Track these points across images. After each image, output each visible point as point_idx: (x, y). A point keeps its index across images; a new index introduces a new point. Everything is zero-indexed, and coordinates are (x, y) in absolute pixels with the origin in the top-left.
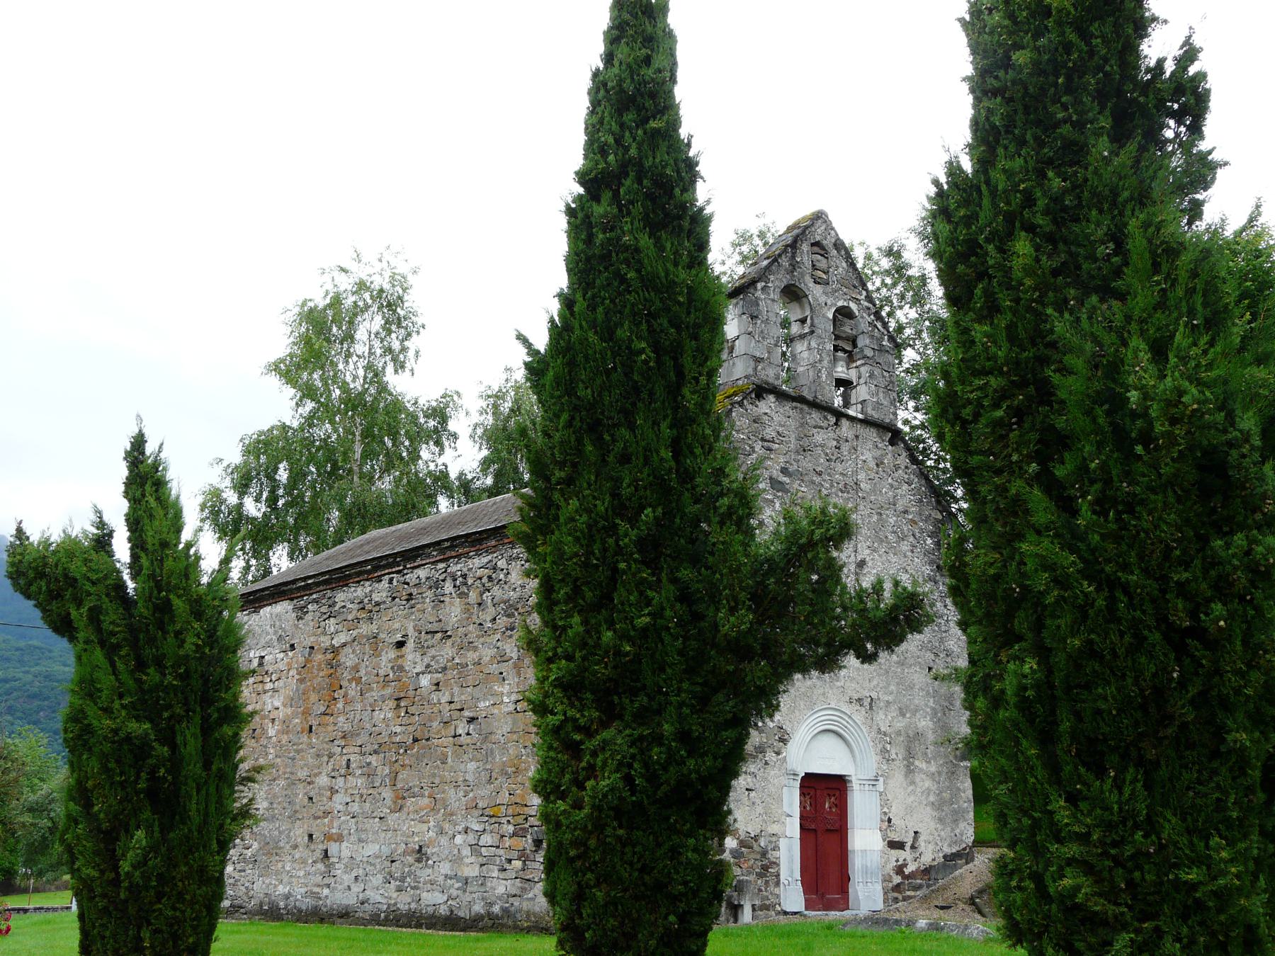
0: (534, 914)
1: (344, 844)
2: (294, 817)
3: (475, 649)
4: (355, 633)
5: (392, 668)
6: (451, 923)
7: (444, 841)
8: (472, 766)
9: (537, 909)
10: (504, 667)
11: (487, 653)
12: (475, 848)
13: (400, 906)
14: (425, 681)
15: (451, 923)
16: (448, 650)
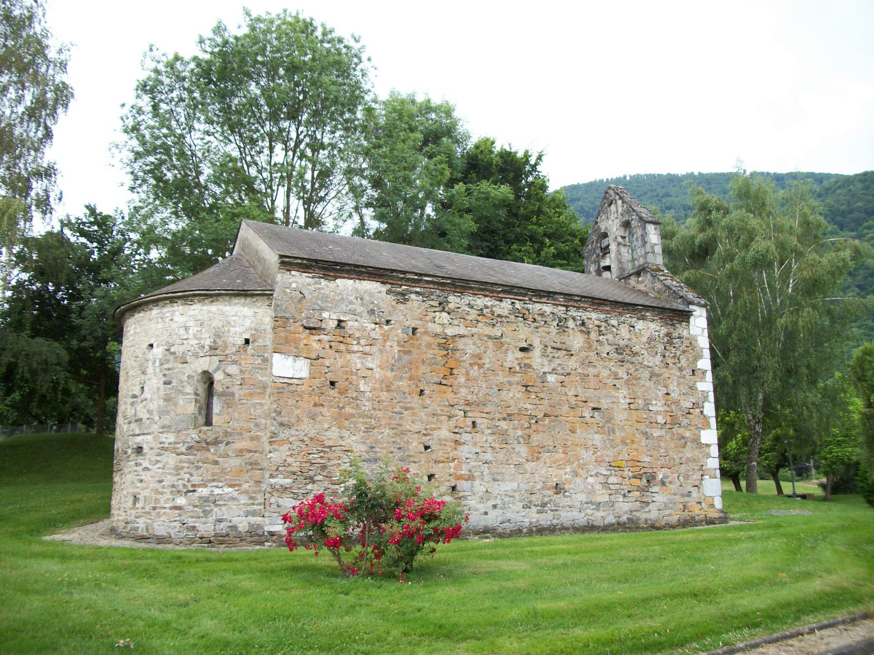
1: (477, 482)
3: (595, 366)
7: (578, 480)
8: (598, 437)
11: (605, 373)
12: (605, 485)
14: (551, 378)
16: (572, 363)
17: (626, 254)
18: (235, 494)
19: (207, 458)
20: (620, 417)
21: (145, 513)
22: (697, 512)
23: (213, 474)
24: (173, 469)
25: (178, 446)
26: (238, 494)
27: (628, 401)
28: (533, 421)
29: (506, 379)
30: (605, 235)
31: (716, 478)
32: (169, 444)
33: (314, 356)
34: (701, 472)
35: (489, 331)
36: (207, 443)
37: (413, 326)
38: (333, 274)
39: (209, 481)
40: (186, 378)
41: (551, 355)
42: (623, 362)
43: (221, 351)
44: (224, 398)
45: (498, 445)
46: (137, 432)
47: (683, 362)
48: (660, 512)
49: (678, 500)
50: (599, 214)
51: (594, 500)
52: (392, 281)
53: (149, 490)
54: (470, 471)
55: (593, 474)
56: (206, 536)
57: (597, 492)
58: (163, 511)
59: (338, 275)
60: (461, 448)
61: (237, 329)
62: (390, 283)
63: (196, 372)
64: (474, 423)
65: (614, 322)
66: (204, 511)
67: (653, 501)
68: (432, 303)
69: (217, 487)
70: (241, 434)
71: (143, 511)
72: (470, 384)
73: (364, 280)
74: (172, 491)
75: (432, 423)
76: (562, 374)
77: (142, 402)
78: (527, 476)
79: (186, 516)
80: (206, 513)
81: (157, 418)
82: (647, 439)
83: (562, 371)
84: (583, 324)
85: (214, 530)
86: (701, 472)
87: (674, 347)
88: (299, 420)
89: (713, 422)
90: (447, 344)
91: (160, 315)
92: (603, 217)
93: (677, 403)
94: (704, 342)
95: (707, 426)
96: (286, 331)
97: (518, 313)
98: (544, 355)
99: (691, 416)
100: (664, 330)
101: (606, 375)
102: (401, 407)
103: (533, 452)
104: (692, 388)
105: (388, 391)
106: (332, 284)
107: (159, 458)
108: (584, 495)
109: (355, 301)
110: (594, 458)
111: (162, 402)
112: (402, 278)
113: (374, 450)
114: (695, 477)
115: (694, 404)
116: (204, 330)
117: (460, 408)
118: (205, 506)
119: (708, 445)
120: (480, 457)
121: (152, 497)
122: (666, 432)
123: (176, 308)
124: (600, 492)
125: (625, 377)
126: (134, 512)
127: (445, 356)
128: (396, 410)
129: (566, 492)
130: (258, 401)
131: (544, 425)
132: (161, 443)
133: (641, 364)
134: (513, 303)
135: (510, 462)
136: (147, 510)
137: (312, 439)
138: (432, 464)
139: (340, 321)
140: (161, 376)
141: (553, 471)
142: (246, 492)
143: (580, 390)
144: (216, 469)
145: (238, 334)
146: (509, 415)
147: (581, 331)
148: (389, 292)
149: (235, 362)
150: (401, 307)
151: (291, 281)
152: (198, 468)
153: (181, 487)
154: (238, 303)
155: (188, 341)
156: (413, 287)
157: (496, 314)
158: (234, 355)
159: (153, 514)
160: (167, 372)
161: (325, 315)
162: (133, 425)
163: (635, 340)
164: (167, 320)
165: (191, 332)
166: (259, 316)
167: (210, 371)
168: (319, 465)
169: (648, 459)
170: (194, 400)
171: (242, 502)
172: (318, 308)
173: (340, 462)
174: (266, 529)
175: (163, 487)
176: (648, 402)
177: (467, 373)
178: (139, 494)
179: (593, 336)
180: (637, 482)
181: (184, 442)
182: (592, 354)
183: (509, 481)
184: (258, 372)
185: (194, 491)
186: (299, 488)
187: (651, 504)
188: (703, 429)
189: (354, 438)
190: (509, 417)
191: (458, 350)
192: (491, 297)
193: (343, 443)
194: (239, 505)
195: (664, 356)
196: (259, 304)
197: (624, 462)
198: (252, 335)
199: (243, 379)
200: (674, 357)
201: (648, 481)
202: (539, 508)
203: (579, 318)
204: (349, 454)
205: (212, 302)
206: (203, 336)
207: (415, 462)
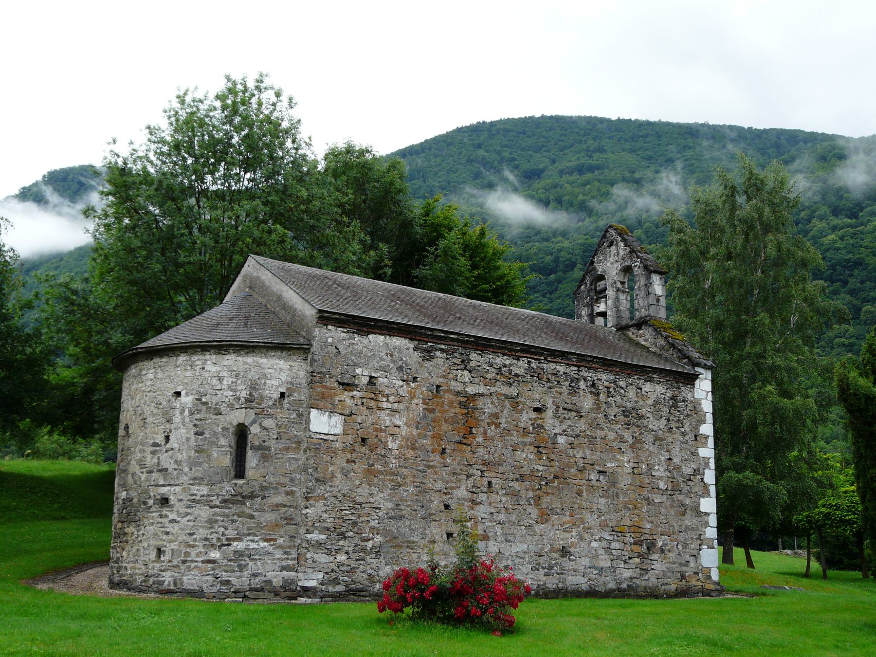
0: (649, 588)
1: (491, 543)
2: (428, 518)
3: (602, 429)
4: (493, 389)
5: (532, 424)
6: (592, 594)
7: (582, 544)
8: (602, 501)
9: (651, 585)
10: (624, 446)
11: (611, 436)
12: (608, 550)
13: (550, 586)
14: (561, 440)
15: (592, 594)
16: (582, 425)
17: (625, 302)
18: (271, 549)
19: (243, 512)
20: (624, 482)
21: (173, 566)
22: (694, 582)
23: (249, 529)
24: (206, 522)
25: (212, 498)
26: (273, 549)
27: (632, 465)
28: (543, 483)
29: (520, 440)
30: (602, 278)
31: (713, 548)
32: (201, 496)
33: (347, 412)
34: (699, 542)
35: (505, 390)
36: (243, 497)
37: (437, 383)
38: (366, 330)
39: (244, 535)
40: (220, 430)
41: (562, 416)
42: (629, 425)
43: (257, 403)
44: (260, 452)
45: (511, 506)
46: (162, 482)
47: (687, 427)
48: (659, 580)
49: (676, 569)
50: (596, 254)
51: (597, 565)
52: (419, 338)
53: (177, 543)
54: (485, 531)
55: (597, 538)
56: (241, 590)
57: (600, 556)
58: (193, 565)
59: (370, 330)
60: (477, 508)
61: (273, 382)
62: (417, 340)
63: (231, 424)
64: (490, 483)
65: (622, 383)
66: (239, 566)
67: (652, 569)
68: (455, 360)
69: (253, 541)
70: (277, 488)
71: (171, 564)
72: (488, 443)
73: (394, 336)
74: (205, 545)
75: (452, 481)
76: (572, 436)
77: (167, 451)
78: (537, 538)
79: (220, 570)
80: (241, 568)
81: (186, 469)
82: (649, 505)
83: (572, 433)
84: (593, 385)
85: (249, 585)
86: (699, 542)
87: (679, 411)
88: (333, 476)
89: (713, 490)
90: (468, 402)
91: (189, 362)
92: (601, 258)
93: (678, 468)
94: (707, 406)
95: (706, 493)
96: (323, 387)
97: (534, 372)
98: (556, 416)
99: (692, 483)
100: (669, 394)
101: (612, 438)
102: (424, 465)
103: (543, 514)
104: (695, 454)
105: (413, 449)
106: (365, 340)
107: (189, 511)
108: (588, 560)
109: (385, 357)
110: (598, 521)
111: (192, 453)
112: (429, 335)
113: (399, 507)
114: (693, 546)
115: (695, 470)
116: (239, 382)
117: (478, 467)
118: (241, 560)
119: (707, 514)
120: (494, 517)
121: (181, 551)
122: (667, 499)
123: (208, 357)
124: (603, 557)
125: (631, 440)
126: (157, 565)
127: (465, 414)
128: (420, 468)
129: (571, 555)
130: (293, 456)
131: (554, 487)
132: (192, 495)
133: (646, 427)
134: (529, 362)
135: (521, 523)
136: (175, 563)
137: (344, 495)
138: (451, 523)
139: (371, 377)
140: (191, 426)
141: (561, 534)
142: (280, 547)
143: (588, 452)
144: (252, 523)
145: (274, 387)
146: (521, 476)
147: (591, 392)
148: (416, 349)
149: (270, 416)
150: (427, 364)
151: (327, 335)
152: (233, 521)
153: (215, 541)
154: (274, 356)
155: (222, 392)
156: (438, 344)
157: (513, 374)
158: (271, 409)
159: (182, 567)
160: (198, 423)
161: (358, 371)
162: (155, 475)
163: (641, 403)
164: (197, 368)
165: (225, 382)
166: (295, 370)
167: (246, 424)
168: (350, 522)
169: (648, 526)
170: (229, 453)
171: (277, 557)
172: (352, 364)
173: (369, 519)
174: (300, 584)
175: (195, 540)
176: (650, 466)
177: (485, 433)
178: (166, 546)
179: (602, 397)
180: (637, 548)
181: (218, 495)
182: (600, 416)
183: (520, 542)
184: (293, 427)
185: (229, 545)
186: (332, 544)
187: (650, 572)
188: (703, 497)
189: (382, 495)
190: (522, 478)
191: (477, 409)
192: (509, 355)
193: (372, 500)
194: (274, 559)
195: (668, 420)
196: (295, 358)
197: (626, 527)
198: (288, 389)
199: (278, 433)
200: (678, 421)
201: (648, 548)
202: (546, 570)
203: (589, 378)
204: (378, 511)
205: (247, 353)
206: (239, 388)
207: (436, 521)
